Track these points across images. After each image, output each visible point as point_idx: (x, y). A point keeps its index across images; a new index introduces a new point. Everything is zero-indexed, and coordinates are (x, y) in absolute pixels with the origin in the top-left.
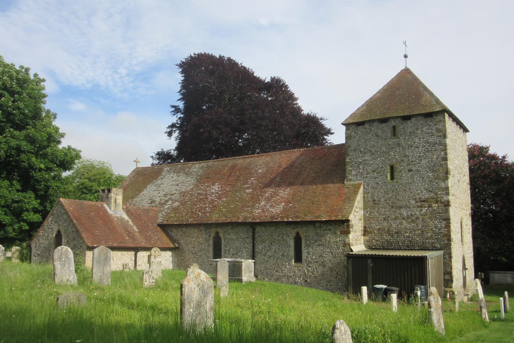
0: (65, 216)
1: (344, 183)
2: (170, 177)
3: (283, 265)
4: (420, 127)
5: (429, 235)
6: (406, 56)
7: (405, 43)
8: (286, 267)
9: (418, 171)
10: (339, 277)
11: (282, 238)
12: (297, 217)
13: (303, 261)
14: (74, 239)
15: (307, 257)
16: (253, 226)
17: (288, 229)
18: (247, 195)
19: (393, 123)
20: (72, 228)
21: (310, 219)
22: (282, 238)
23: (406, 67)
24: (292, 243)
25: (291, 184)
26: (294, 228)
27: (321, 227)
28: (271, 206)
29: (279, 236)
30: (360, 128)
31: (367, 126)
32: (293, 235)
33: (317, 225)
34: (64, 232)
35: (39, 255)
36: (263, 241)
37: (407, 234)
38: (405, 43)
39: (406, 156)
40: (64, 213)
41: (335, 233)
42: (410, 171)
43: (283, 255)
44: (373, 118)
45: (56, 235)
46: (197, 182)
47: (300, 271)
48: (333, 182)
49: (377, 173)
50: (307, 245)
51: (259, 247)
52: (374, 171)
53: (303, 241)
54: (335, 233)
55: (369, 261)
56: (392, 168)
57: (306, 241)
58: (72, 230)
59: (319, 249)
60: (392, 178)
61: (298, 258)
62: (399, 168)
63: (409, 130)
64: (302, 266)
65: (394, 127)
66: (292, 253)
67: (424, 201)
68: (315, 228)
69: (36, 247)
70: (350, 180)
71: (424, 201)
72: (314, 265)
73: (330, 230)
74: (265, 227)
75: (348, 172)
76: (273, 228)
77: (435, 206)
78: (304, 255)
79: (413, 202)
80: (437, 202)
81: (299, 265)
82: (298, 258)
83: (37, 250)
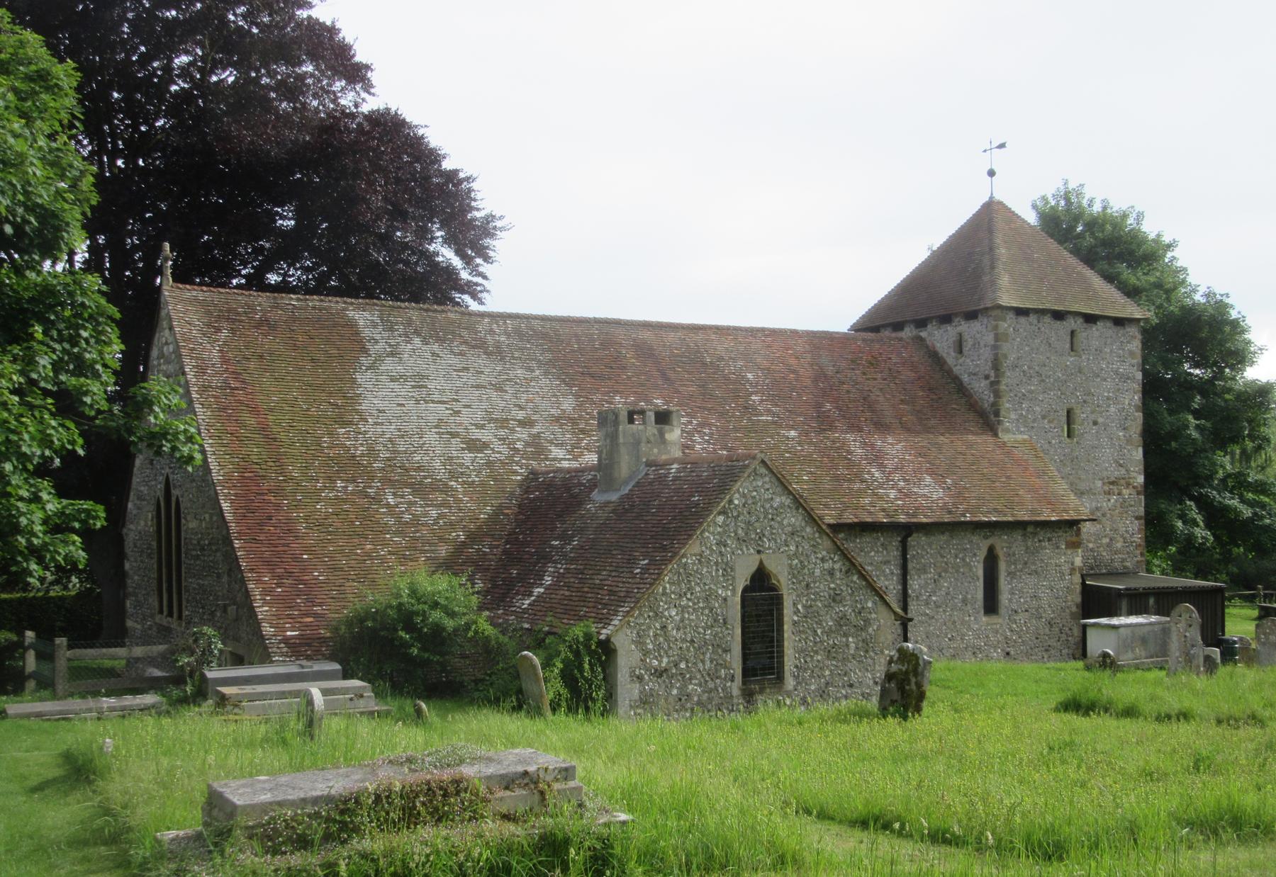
0: (793, 519)
1: (996, 435)
2: (428, 355)
3: (963, 622)
4: (1109, 341)
5: (1119, 545)
6: (991, 173)
7: (1002, 146)
8: (969, 628)
9: (1106, 426)
10: (1064, 637)
11: (963, 559)
12: (996, 510)
13: (1002, 611)
14: (836, 598)
15: (1010, 600)
16: (904, 532)
17: (975, 539)
18: (800, 444)
19: (1071, 323)
20: (823, 560)
21: (1026, 518)
22: (963, 559)
23: (991, 197)
24: (980, 573)
25: (882, 427)
26: (986, 537)
27: (1035, 534)
28: (905, 480)
29: (956, 557)
30: (1022, 320)
31: (1033, 318)
32: (982, 554)
33: (1030, 529)
34: (795, 573)
35: (659, 673)
36: (923, 570)
37: (1091, 545)
38: (1002, 146)
39: (1089, 394)
40: (782, 505)
41: (1058, 548)
42: (1095, 423)
43: (964, 601)
44: (1048, 306)
45: (745, 590)
46: (567, 385)
47: (997, 632)
48: (973, 433)
49: (1049, 422)
50: (1009, 574)
51: (914, 584)
52: (1044, 417)
53: (1002, 566)
54: (1058, 548)
55: (1152, 601)
56: (1069, 413)
57: (1009, 563)
58: (826, 566)
59: (1032, 580)
60: (1069, 436)
61: (991, 606)
62: (1081, 415)
63: (1095, 343)
64: (1000, 621)
65: (1073, 333)
66: (980, 595)
67: (1112, 483)
68: (1024, 535)
69: (640, 642)
70: (1007, 431)
71: (1112, 483)
72: (1021, 617)
73: (1049, 540)
74: (926, 534)
75: (1003, 413)
76: (944, 538)
77: (1126, 492)
78: (1004, 598)
79: (1099, 484)
80: (1128, 484)
81: (994, 619)
82: (991, 606)
83: (646, 653)
